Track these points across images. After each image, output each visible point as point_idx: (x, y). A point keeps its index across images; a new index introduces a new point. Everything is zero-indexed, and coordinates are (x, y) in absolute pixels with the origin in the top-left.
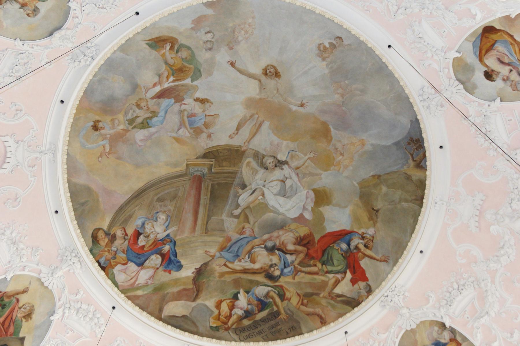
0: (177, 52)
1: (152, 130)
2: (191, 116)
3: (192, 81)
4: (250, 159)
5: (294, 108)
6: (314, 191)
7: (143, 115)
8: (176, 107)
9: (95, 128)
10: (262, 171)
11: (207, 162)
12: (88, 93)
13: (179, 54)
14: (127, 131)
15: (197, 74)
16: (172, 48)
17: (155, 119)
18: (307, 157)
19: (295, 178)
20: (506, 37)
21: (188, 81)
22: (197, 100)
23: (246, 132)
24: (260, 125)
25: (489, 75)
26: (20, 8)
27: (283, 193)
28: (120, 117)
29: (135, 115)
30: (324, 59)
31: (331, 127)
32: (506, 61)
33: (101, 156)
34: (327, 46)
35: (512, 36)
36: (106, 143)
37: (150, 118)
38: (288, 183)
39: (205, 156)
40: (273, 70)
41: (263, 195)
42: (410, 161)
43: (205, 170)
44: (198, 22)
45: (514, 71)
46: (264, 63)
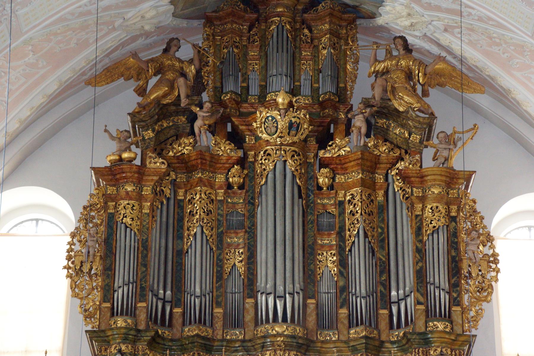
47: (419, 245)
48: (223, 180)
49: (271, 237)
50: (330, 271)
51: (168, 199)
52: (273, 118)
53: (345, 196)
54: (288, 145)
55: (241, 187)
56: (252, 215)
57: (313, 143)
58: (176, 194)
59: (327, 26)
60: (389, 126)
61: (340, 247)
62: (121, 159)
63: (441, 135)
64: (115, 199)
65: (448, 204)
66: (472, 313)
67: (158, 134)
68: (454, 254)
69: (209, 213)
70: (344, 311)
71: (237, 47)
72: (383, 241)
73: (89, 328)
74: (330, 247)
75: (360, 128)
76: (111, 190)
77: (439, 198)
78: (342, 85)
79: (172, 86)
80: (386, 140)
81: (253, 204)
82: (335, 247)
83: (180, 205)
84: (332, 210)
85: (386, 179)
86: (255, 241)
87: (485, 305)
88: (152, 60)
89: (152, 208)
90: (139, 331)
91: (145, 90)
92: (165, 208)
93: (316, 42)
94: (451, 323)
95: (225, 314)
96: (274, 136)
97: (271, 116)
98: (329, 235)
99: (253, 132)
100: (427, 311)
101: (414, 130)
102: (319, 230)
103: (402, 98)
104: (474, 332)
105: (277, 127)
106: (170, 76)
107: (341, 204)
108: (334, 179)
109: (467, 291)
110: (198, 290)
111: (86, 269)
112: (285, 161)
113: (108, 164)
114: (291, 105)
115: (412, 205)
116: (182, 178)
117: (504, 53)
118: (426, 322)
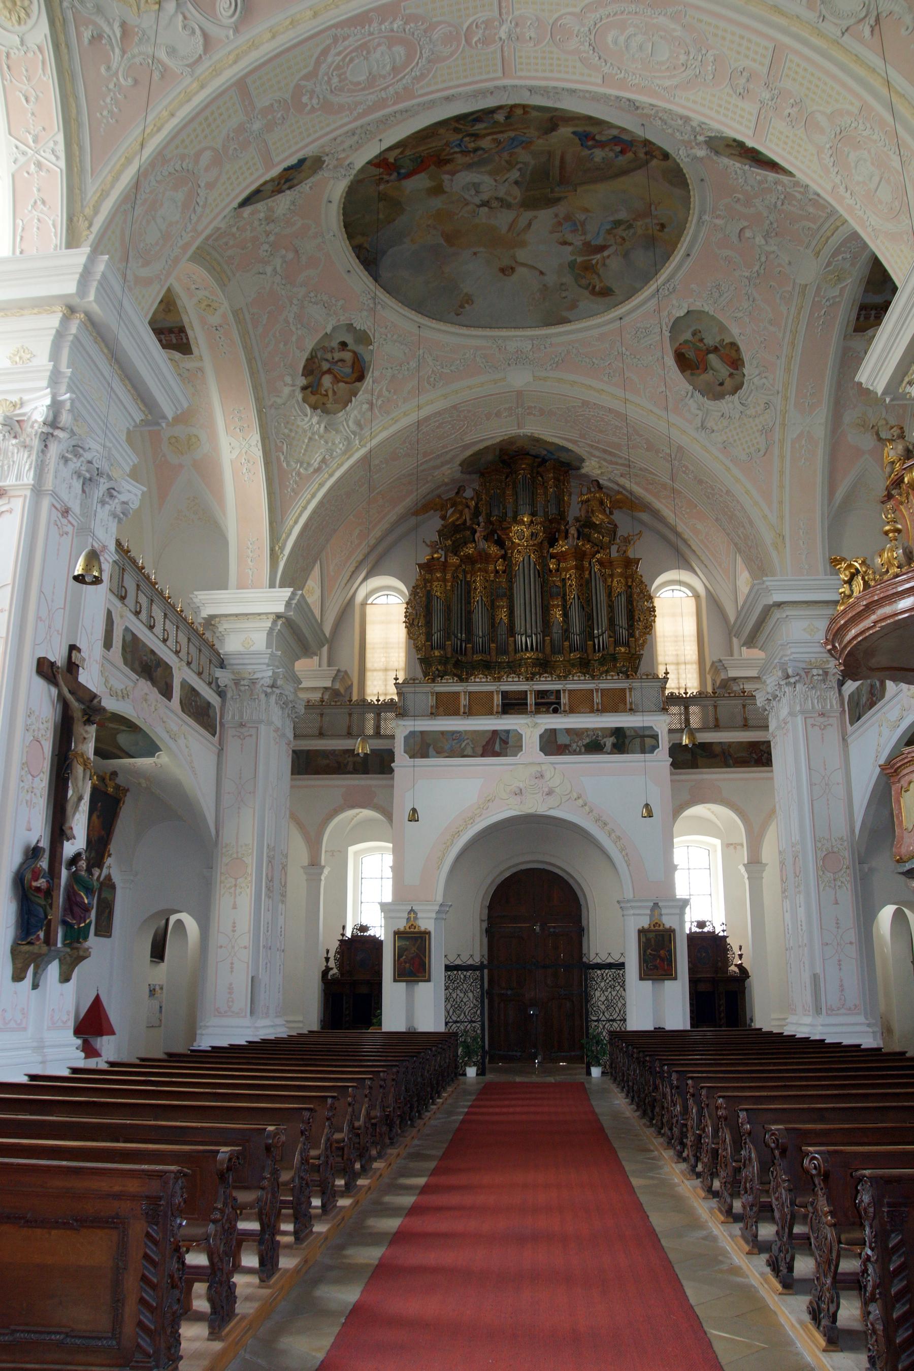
0: (590, 284)
1: (612, 219)
2: (575, 231)
3: (575, 260)
4: (513, 202)
5: (482, 249)
6: (444, 192)
7: (620, 231)
8: (589, 237)
9: (663, 226)
10: (501, 194)
11: (557, 195)
12: (667, 257)
13: (588, 282)
14: (634, 220)
15: (572, 265)
16: (594, 287)
17: (608, 227)
18: (461, 214)
19: (467, 197)
20: (348, 380)
21: (579, 259)
22: (570, 244)
23: (522, 222)
24: (509, 229)
25: (344, 345)
27: (476, 186)
28: (640, 232)
29: (627, 232)
30: (466, 294)
31: (445, 244)
32: (339, 364)
33: (659, 203)
34: (466, 305)
35: (346, 383)
36: (654, 213)
37: (612, 228)
38: (473, 192)
39: (558, 200)
40: (507, 273)
41: (496, 181)
42: (368, 247)
43: (557, 189)
44: (573, 306)
45: (331, 360)
46: (515, 277)
47: (610, 603)
48: (493, 568)
49: (522, 601)
51: (461, 581)
53: (566, 575)
55: (504, 572)
56: (511, 589)
57: (546, 544)
58: (465, 577)
59: (552, 475)
60: (590, 533)
62: (433, 558)
63: (621, 538)
64: (430, 581)
65: (626, 578)
66: (641, 642)
67: (454, 542)
68: (630, 607)
69: (485, 588)
70: (566, 644)
71: (499, 489)
72: (589, 601)
73: (419, 656)
74: (558, 606)
75: (573, 535)
76: (428, 576)
77: (621, 575)
78: (562, 509)
79: (461, 513)
80: (589, 541)
81: (511, 582)
83: (468, 584)
84: (559, 584)
85: (590, 564)
86: (514, 604)
87: (648, 636)
88: (449, 499)
89: (452, 586)
90: (447, 658)
91: (446, 517)
92: (459, 586)
93: (546, 484)
94: (629, 647)
95: (497, 648)
98: (557, 599)
99: (510, 539)
100: (615, 641)
102: (552, 596)
103: (597, 516)
104: (642, 652)
106: (460, 507)
107: (564, 580)
108: (559, 565)
109: (638, 629)
110: (480, 633)
111: (416, 623)
112: (530, 556)
113: (426, 561)
114: (532, 522)
115: (606, 579)
116: (468, 568)
118: (615, 648)
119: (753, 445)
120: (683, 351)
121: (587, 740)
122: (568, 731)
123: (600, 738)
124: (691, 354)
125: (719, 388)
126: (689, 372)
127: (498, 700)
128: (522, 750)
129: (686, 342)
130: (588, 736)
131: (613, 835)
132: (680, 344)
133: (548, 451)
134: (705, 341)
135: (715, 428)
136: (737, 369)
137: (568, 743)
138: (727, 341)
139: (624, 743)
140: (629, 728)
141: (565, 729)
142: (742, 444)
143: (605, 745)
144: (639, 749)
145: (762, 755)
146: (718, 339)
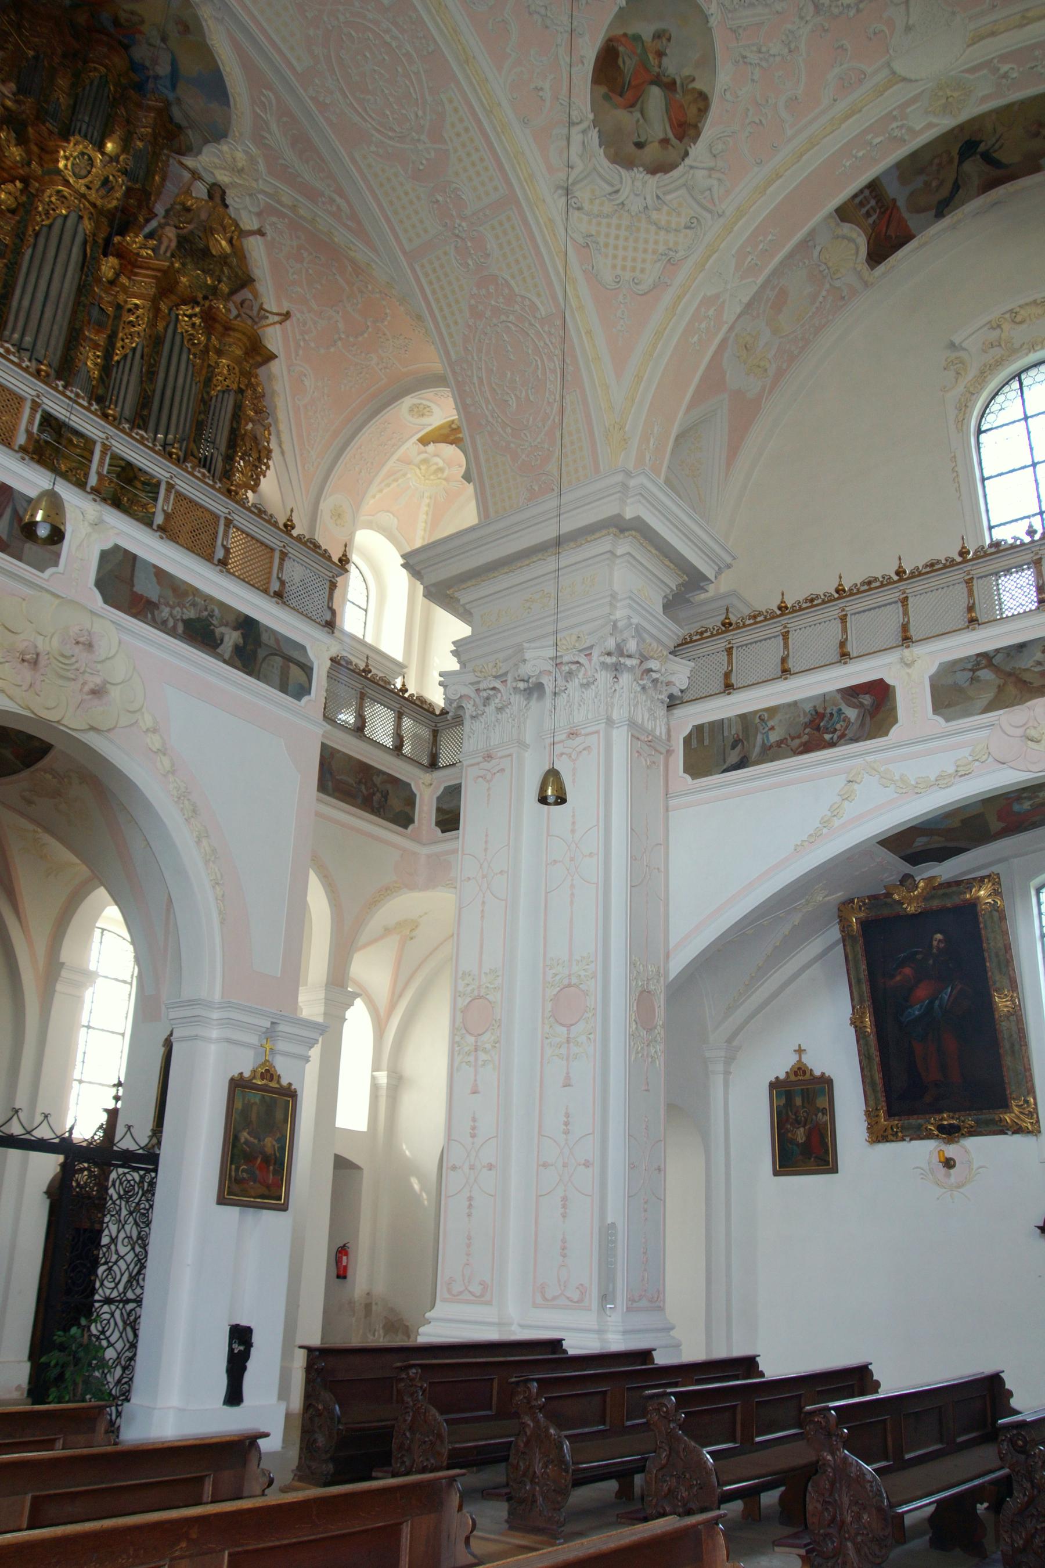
26: (666, 55)
50: (88, 372)
52: (90, 158)
54: (88, 201)
61: (107, 351)
74: (96, 346)
81: (22, 240)
82: (101, 349)
96: (80, 181)
97: (89, 156)
101: (225, 279)
105: (89, 172)
112: (81, 217)
117: (292, 274)
119: (633, 269)
120: (621, 49)
121: (191, 614)
122: (160, 574)
123: (215, 622)
124: (628, 64)
125: (632, 149)
126: (603, 90)
127: (31, 421)
128: (56, 564)
129: (637, 38)
130: (194, 605)
131: (205, 843)
132: (625, 35)
133: (174, 76)
134: (665, 61)
135: (586, 206)
136: (680, 139)
137: (154, 598)
138: (698, 85)
139: (255, 653)
140: (268, 629)
141: (155, 566)
142: (615, 257)
143: (222, 641)
144: (277, 680)
145: (374, 794)
146: (686, 72)
